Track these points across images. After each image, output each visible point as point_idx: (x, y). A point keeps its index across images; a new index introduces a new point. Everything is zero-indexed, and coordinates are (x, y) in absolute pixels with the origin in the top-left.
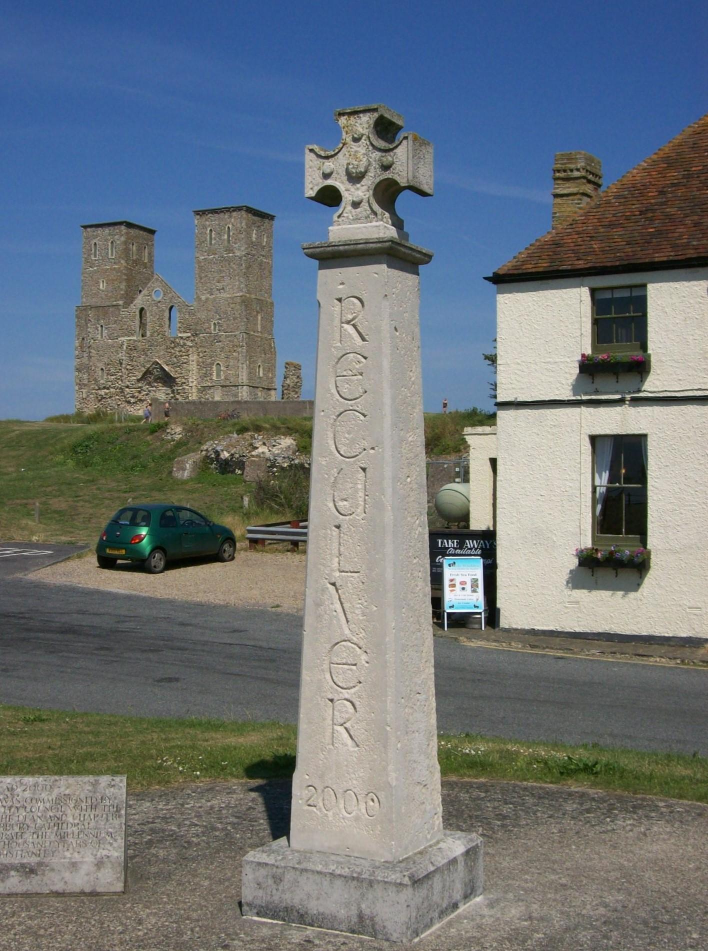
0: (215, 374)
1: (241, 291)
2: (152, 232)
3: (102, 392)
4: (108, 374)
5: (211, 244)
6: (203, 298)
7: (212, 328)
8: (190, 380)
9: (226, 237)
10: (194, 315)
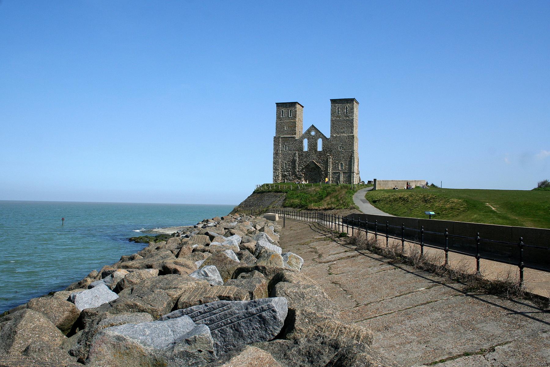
2: (303, 107)
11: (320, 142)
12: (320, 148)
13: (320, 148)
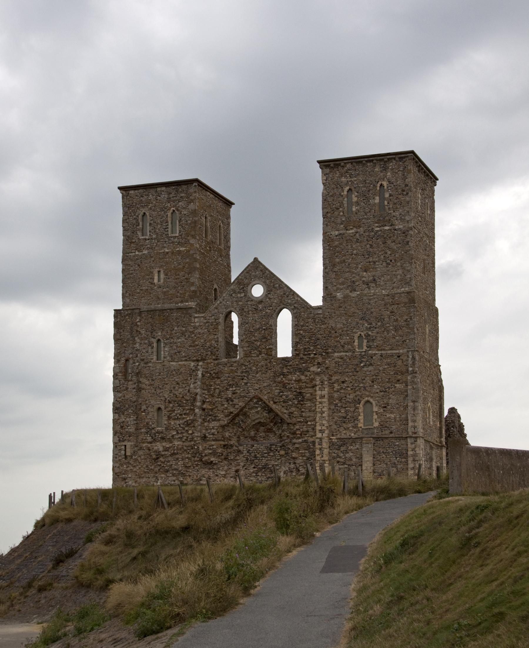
0: (361, 418)
1: (408, 284)
3: (159, 446)
4: (169, 418)
5: (350, 210)
6: (339, 295)
7: (356, 343)
8: (318, 428)
9: (377, 200)
10: (323, 323)
11: (285, 320)
12: (284, 348)
13: (284, 348)
